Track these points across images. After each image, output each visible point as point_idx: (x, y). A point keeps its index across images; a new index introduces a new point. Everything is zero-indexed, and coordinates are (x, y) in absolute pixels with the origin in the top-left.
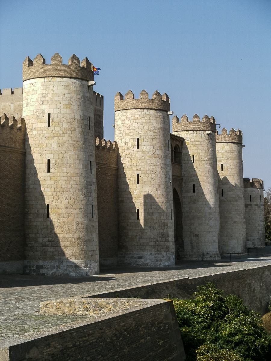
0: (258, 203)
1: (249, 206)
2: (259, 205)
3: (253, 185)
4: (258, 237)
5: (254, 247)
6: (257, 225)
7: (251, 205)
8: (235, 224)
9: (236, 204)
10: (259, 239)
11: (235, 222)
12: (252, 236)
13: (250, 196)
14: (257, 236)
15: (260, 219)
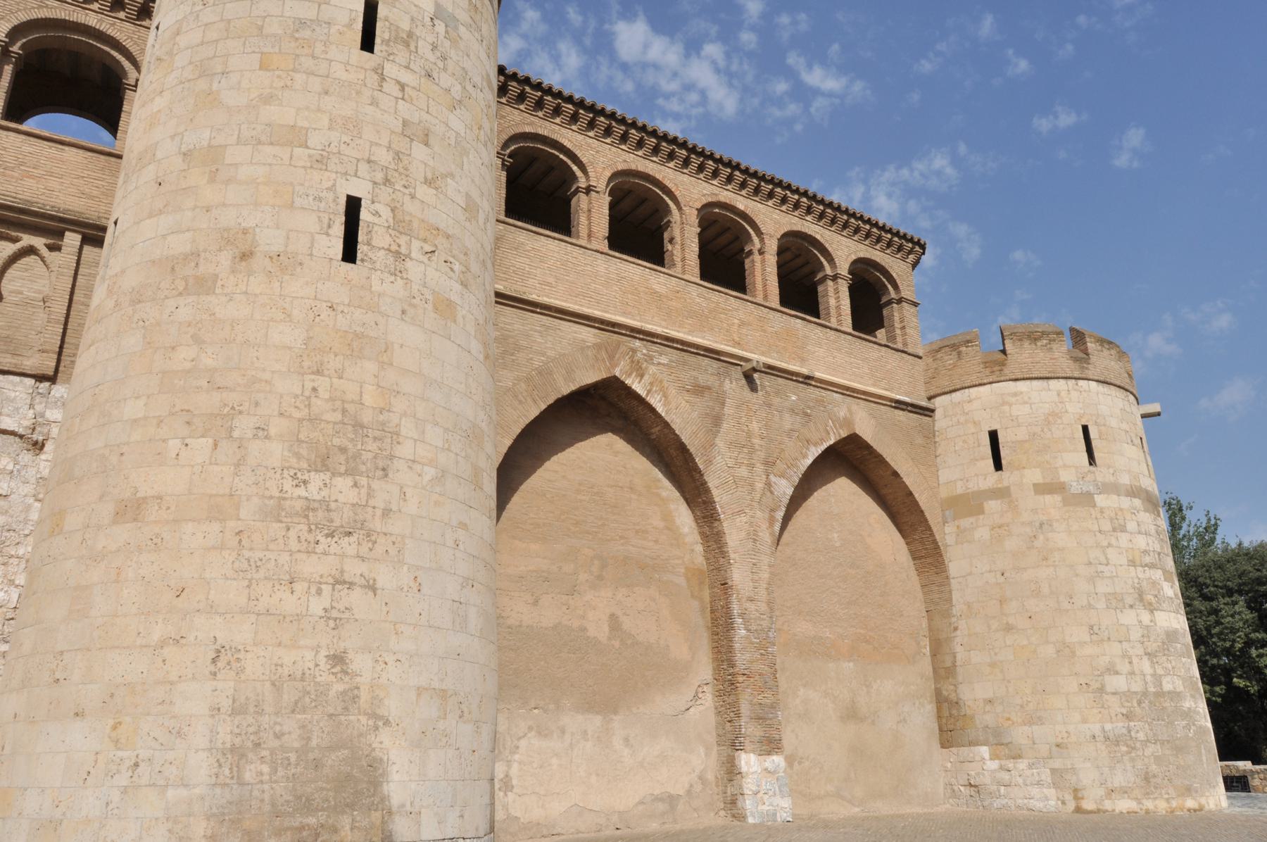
0: (1066, 476)
1: (992, 505)
2: (1075, 488)
3: (1004, 365)
4: (1096, 728)
5: (1071, 806)
6: (1076, 634)
7: (1001, 493)
8: (122, 533)
9: (185, 313)
10: (1112, 741)
11: (131, 510)
12: (1040, 721)
13: (993, 436)
14: (1084, 721)
15: (1103, 587)
